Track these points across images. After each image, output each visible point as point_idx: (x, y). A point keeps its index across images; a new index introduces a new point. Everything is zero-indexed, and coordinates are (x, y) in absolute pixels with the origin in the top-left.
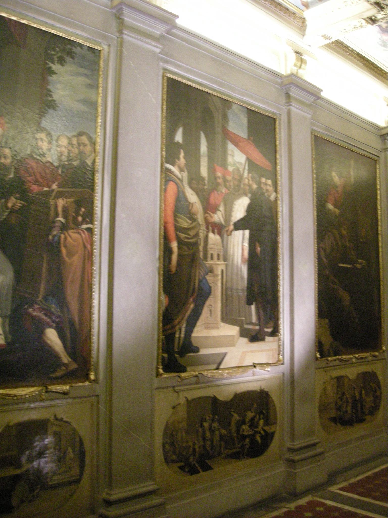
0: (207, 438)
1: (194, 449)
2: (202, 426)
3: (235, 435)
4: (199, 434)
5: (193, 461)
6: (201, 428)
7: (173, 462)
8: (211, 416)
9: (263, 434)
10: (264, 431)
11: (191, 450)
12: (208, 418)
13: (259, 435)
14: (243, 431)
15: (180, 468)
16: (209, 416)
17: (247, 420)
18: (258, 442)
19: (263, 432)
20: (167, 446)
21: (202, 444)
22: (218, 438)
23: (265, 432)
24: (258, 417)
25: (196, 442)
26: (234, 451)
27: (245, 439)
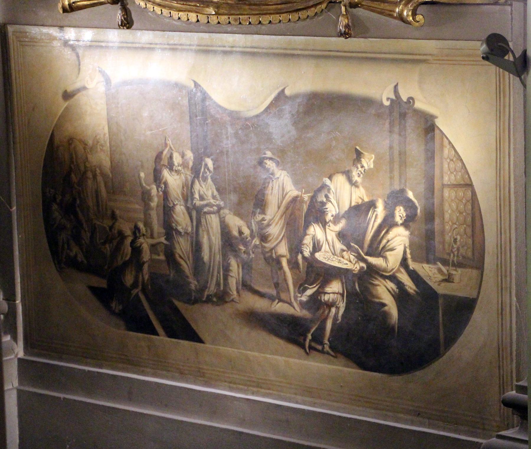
0: (179, 228)
1: (137, 251)
2: (157, 177)
3: (283, 250)
4: (153, 204)
5: (135, 285)
6: (158, 187)
7: (74, 264)
8: (190, 155)
9: (411, 291)
10: (414, 276)
11: (128, 249)
12: (177, 159)
13: (391, 285)
14: (317, 248)
15: (94, 290)
16: (183, 156)
17: (331, 210)
18: (386, 315)
19: (404, 278)
20: (57, 214)
21: (163, 240)
22: (217, 240)
23: (417, 285)
24: (380, 211)
25: (141, 225)
26: (279, 307)
27: (326, 282)
